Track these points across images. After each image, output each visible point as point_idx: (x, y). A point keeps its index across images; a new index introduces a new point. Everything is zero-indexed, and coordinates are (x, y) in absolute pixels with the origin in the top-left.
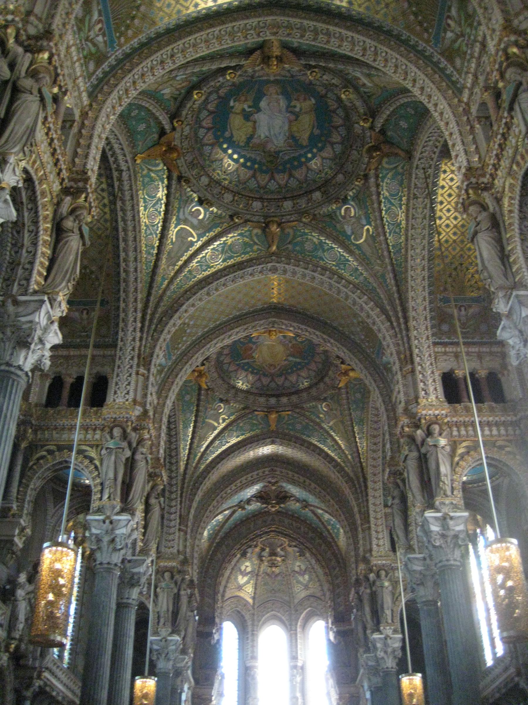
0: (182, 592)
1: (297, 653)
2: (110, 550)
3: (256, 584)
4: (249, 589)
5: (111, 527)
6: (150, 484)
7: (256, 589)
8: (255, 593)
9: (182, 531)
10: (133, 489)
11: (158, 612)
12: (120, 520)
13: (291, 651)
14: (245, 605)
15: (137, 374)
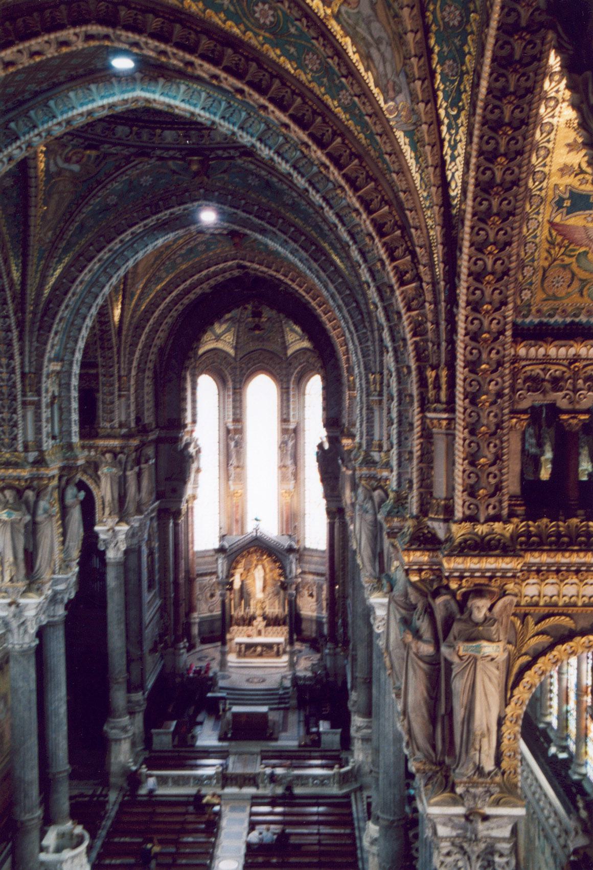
0: (128, 473)
1: (288, 414)
2: (22, 631)
3: (238, 331)
4: (229, 338)
5: (18, 610)
6: (65, 479)
7: (238, 337)
8: (237, 343)
9: (124, 396)
10: (40, 556)
11: (102, 497)
12: (27, 605)
13: (282, 414)
14: (225, 358)
15: (24, 403)
